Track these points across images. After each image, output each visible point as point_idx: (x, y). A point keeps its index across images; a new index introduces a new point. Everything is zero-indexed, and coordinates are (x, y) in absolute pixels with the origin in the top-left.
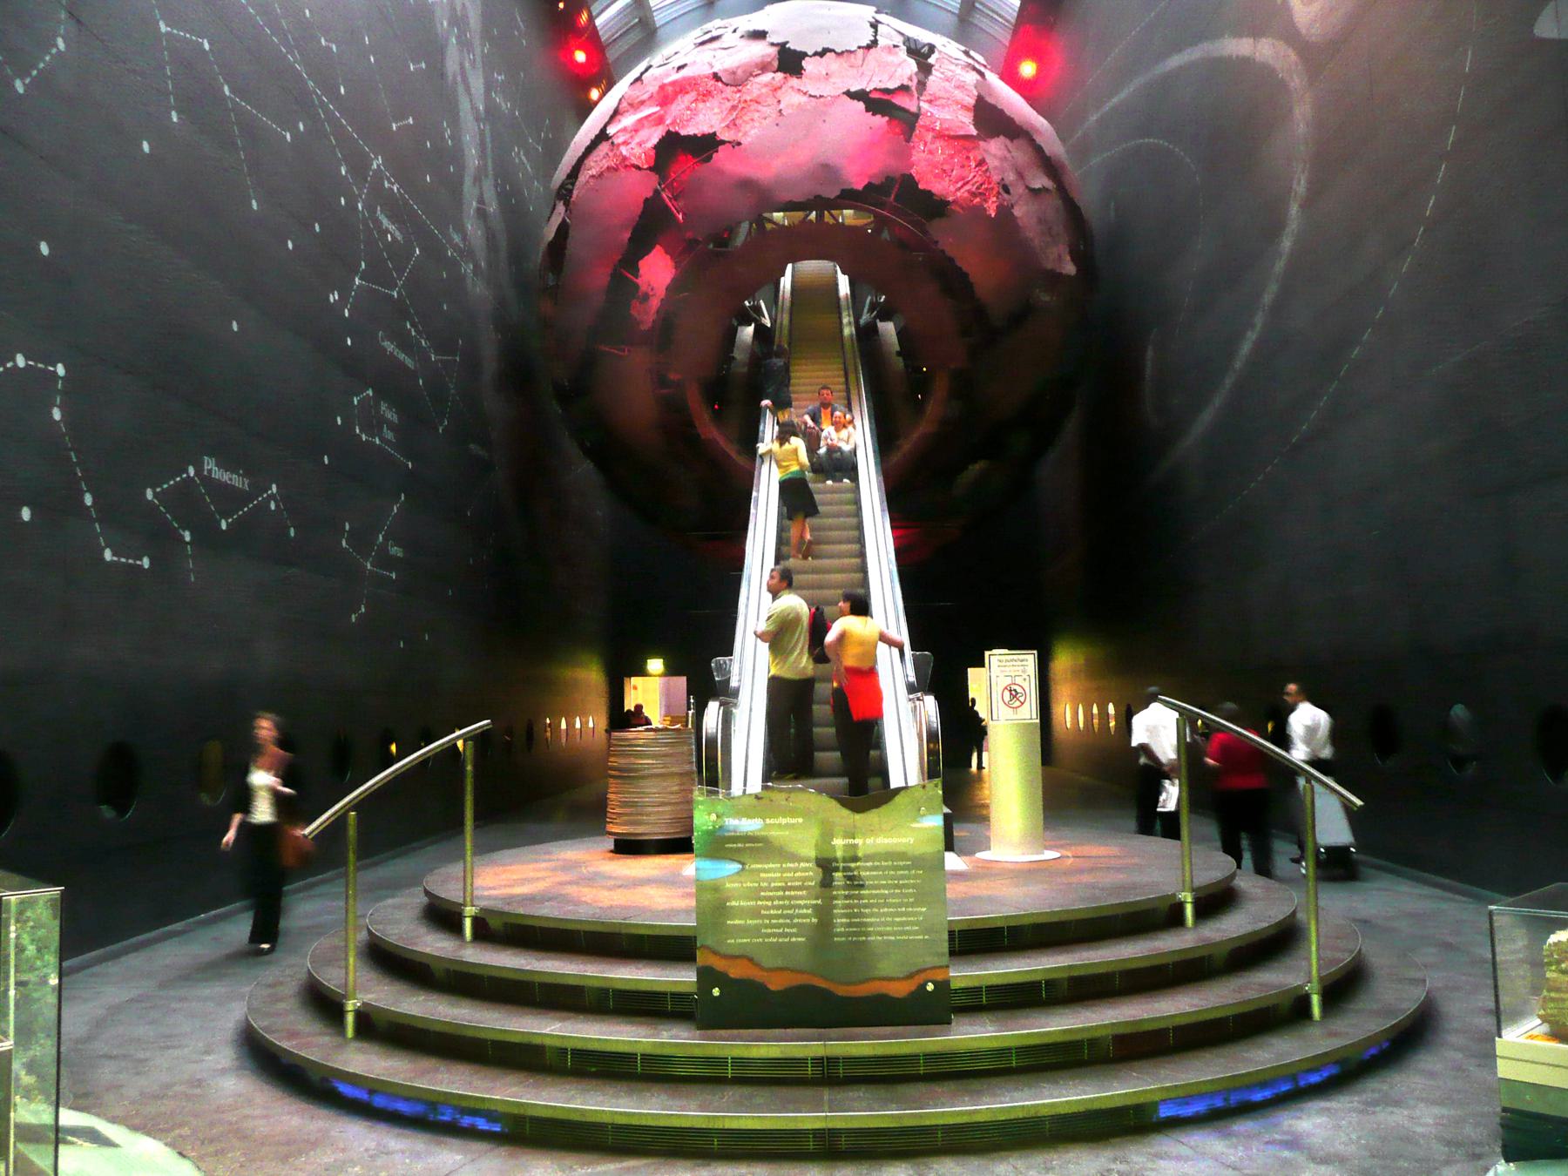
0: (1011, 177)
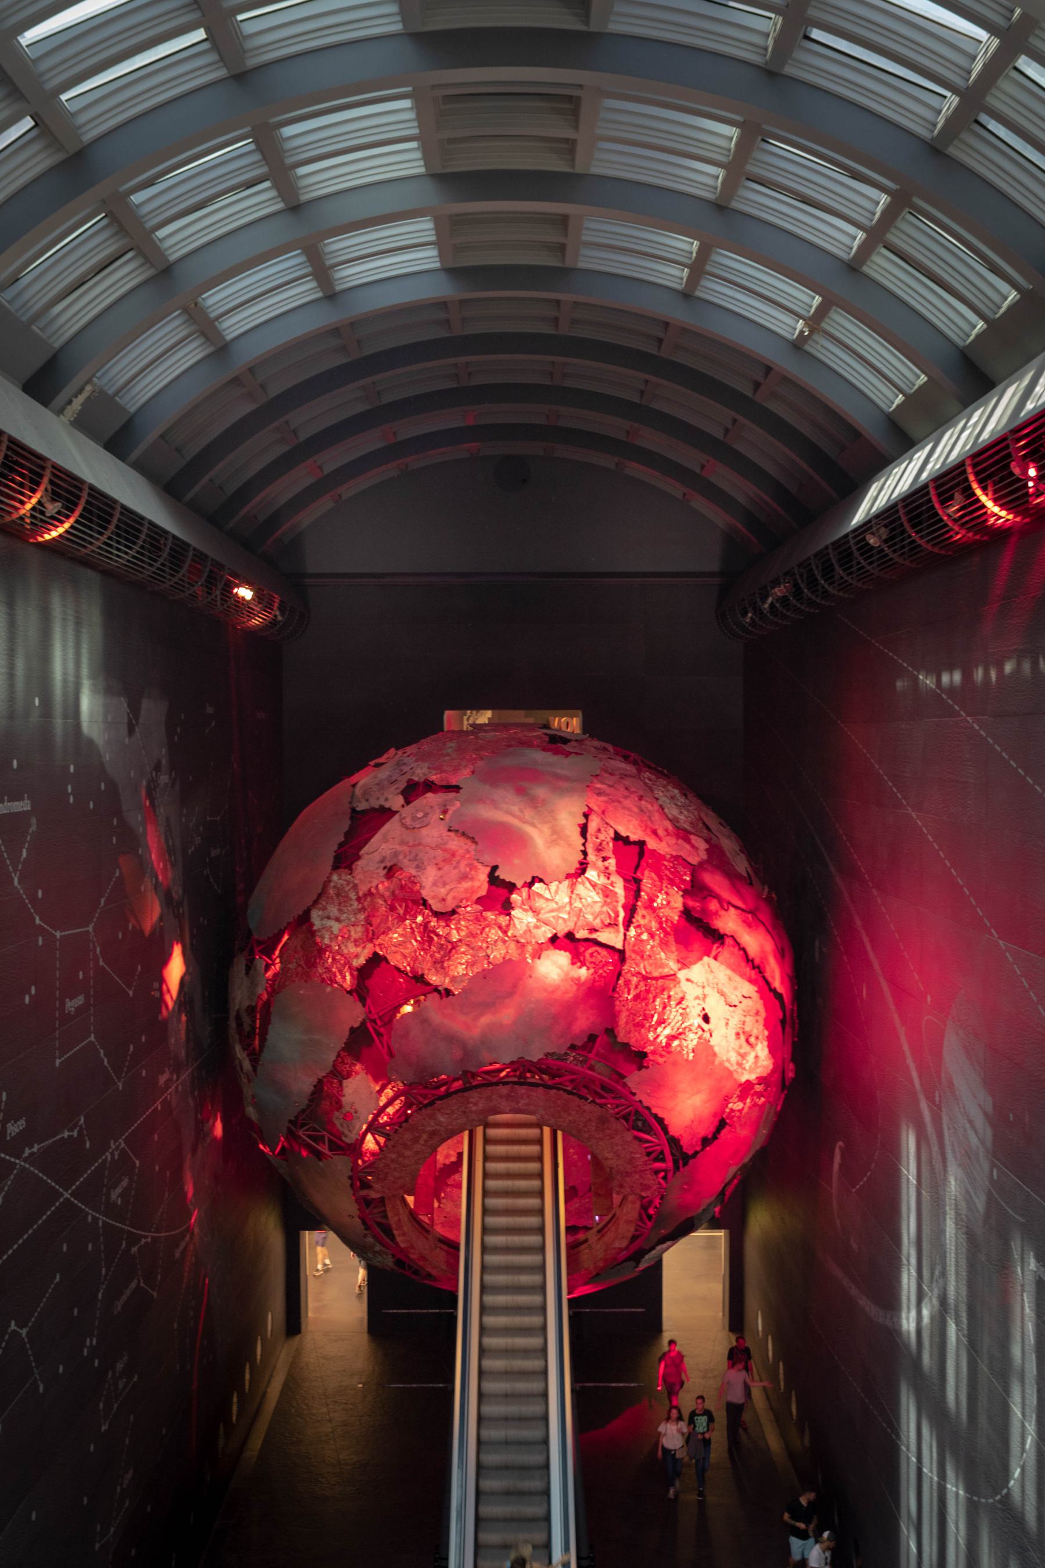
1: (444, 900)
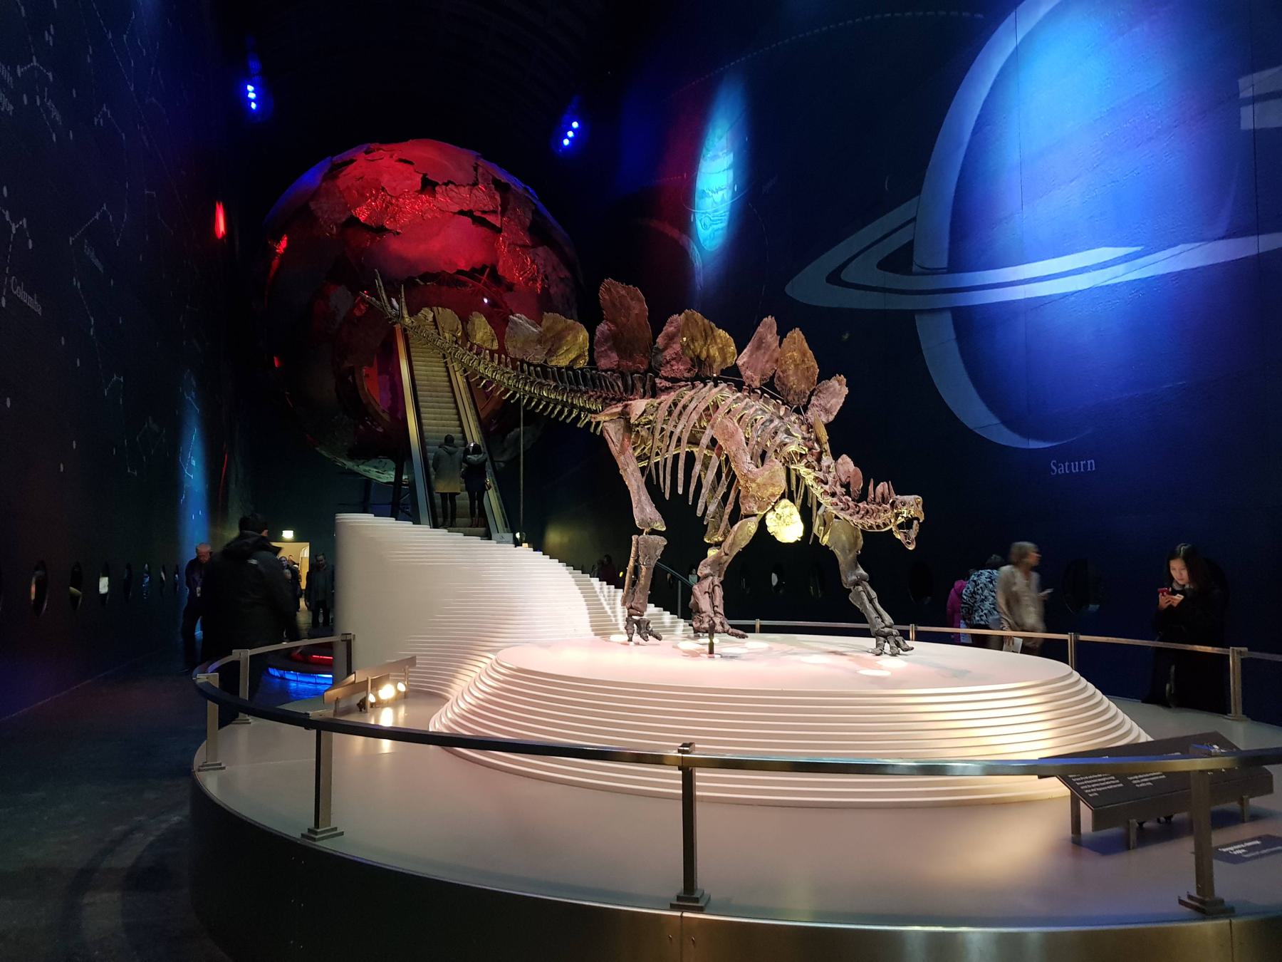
0: (550, 269)
1: (395, 189)
